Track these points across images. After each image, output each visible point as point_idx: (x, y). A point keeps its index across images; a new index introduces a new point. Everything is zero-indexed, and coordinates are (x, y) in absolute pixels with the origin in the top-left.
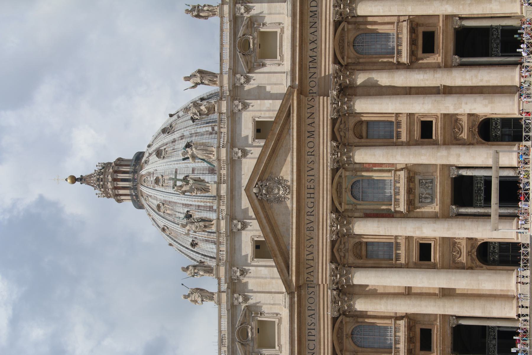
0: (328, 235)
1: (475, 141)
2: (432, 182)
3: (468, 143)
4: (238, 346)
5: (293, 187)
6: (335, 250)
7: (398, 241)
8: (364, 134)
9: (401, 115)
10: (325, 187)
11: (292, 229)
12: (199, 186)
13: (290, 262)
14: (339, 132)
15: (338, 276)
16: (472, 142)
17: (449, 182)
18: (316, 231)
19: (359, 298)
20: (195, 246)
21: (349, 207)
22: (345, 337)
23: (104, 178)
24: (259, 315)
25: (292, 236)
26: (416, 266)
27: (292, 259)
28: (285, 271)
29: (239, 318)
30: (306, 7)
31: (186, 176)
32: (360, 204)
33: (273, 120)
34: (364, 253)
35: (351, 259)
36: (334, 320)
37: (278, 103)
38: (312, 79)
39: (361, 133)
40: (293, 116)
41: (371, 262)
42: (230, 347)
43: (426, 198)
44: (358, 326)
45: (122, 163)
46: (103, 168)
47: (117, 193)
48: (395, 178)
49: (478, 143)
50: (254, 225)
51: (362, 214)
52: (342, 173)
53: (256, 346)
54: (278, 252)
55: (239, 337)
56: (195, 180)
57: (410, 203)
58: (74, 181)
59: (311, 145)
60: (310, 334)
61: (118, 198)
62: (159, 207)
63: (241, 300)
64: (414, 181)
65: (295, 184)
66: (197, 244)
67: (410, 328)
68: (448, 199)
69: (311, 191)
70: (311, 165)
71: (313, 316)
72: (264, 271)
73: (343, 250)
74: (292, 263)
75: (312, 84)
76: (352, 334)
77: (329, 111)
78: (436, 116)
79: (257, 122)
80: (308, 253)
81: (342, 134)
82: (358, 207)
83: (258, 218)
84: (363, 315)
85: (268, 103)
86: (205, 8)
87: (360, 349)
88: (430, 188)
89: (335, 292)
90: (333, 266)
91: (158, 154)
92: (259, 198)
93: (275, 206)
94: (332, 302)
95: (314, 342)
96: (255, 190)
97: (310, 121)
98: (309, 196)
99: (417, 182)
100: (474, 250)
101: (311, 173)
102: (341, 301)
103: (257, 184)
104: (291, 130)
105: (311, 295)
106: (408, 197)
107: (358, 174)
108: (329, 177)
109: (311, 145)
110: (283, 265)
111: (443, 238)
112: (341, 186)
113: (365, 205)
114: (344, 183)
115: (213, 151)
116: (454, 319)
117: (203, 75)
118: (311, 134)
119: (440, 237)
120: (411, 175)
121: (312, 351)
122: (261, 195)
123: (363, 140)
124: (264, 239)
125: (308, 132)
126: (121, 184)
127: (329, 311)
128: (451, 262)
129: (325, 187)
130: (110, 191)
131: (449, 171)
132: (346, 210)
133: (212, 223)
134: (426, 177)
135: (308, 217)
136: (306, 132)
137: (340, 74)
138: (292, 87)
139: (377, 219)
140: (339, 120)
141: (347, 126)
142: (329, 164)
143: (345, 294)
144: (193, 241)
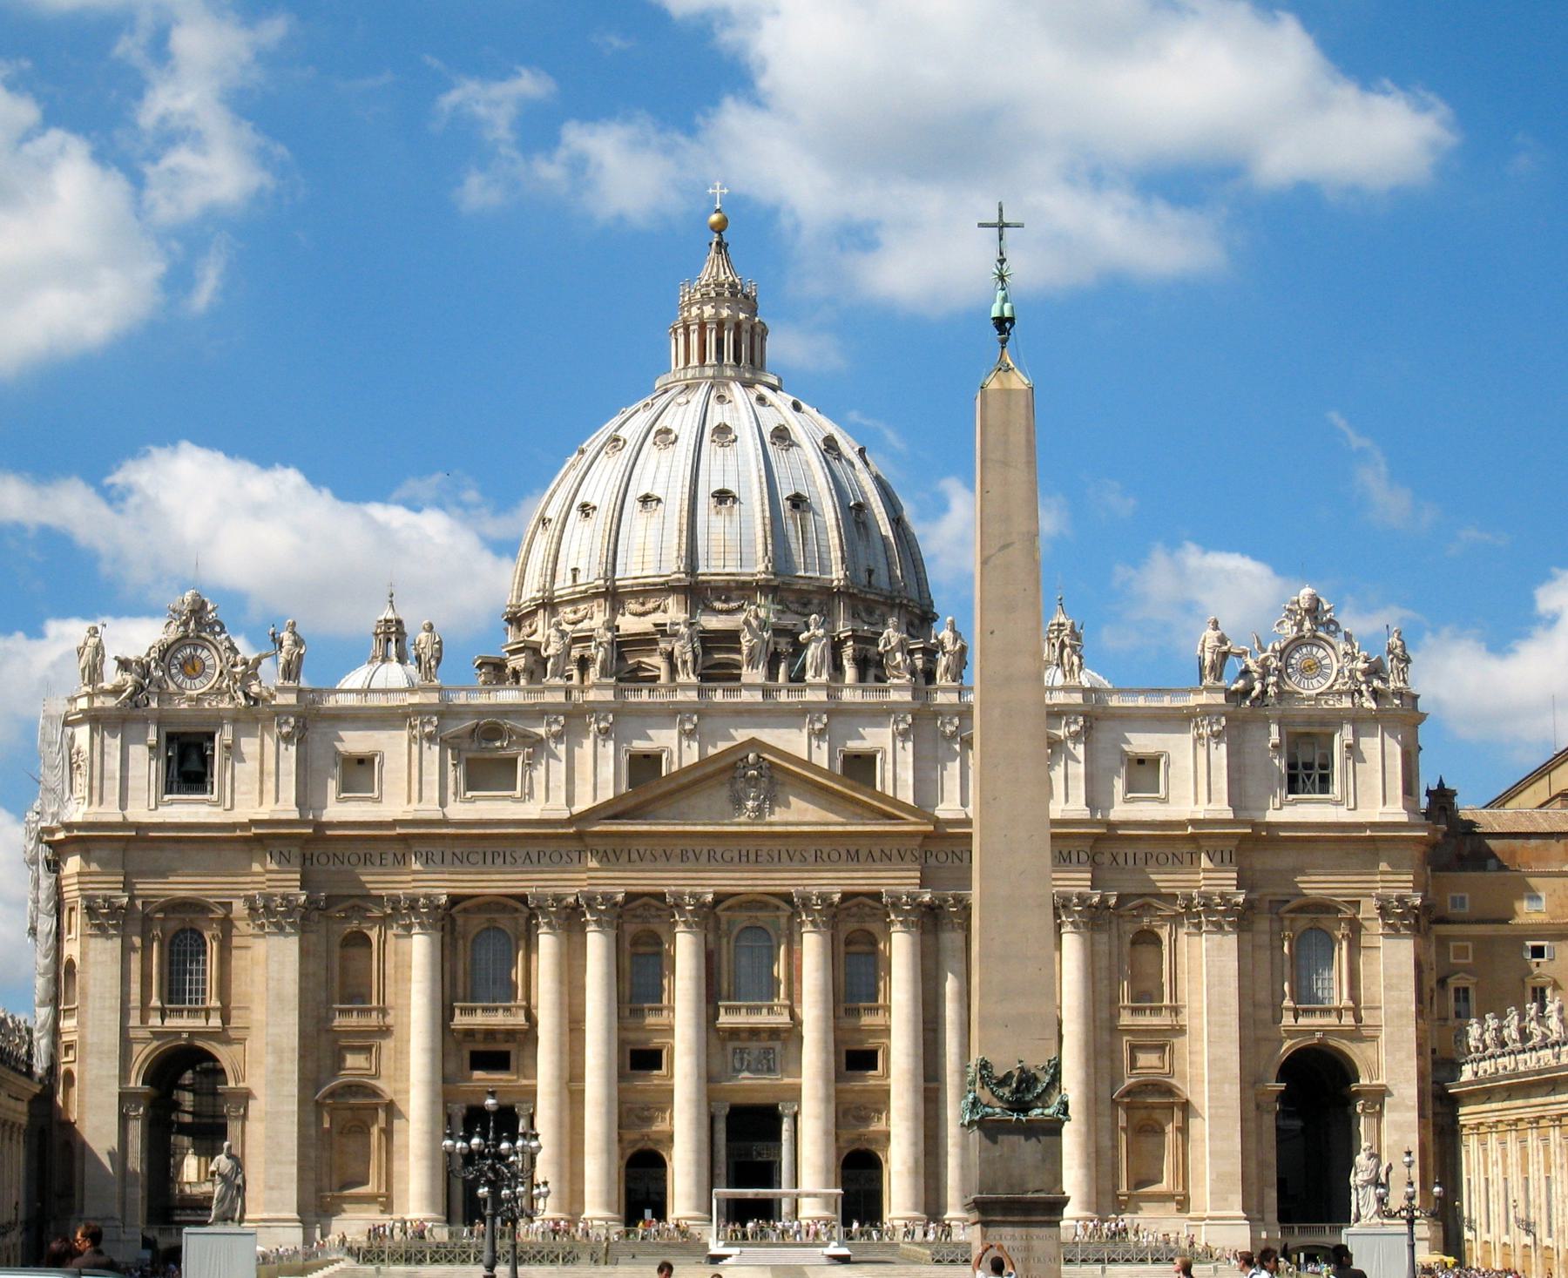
0: (673, 888)
1: (842, 1144)
2: (770, 1070)
3: (839, 1131)
4: (470, 723)
5: (758, 825)
6: (645, 899)
7: (665, 1013)
8: (853, 949)
9: (887, 1014)
10: (760, 882)
11: (684, 824)
12: (757, 651)
13: (625, 821)
14: (857, 905)
15: (603, 907)
16: (841, 1140)
17: (770, 1101)
18: (682, 866)
19: (561, 945)
20: (583, 511)
21: (724, 926)
22: (489, 916)
23: (726, 300)
24: (526, 762)
25: (672, 824)
26: (622, 1043)
27: (632, 824)
28: (610, 812)
29: (520, 725)
30: (1076, 844)
31: (734, 497)
32: (728, 943)
33: (879, 788)
34: (642, 949)
35: (631, 928)
36: (522, 899)
37: (907, 796)
38: (950, 855)
39: (855, 943)
40: (885, 824)
41: (627, 963)
42: (468, 709)
43: (742, 1059)
44: (509, 938)
45: (757, 340)
46: (746, 297)
47: (692, 328)
48: (777, 1005)
49: (838, 1149)
50: (692, 755)
51: (711, 946)
52: (784, 910)
53: (470, 755)
54: (642, 798)
55: (485, 724)
56: (768, 642)
57: (734, 1033)
58: (716, 229)
59: (835, 856)
60: (496, 854)
61: (681, 331)
62: (668, 431)
63: (555, 728)
64: (772, 1040)
65: (766, 829)
66: (587, 515)
67: (511, 1034)
68: (740, 1099)
69: (752, 857)
70: (797, 857)
71: (528, 861)
72: (607, 771)
73: (646, 913)
74: (623, 824)
75: (942, 857)
76: (495, 928)
77: (894, 888)
78: (887, 1074)
79: (874, 757)
80: (642, 852)
81: (854, 910)
82: (724, 941)
83: (704, 761)
84: (531, 947)
85: (907, 776)
86: (1075, 659)
87: (469, 944)
88: (760, 1066)
89: (571, 900)
90: (620, 897)
91: (781, 430)
92: (739, 763)
93: (724, 793)
94: (555, 895)
95: (481, 862)
96: (751, 756)
97: (877, 854)
98: (744, 852)
99: (769, 1044)
100: (651, 1145)
101: (784, 856)
102: (557, 911)
103: (764, 759)
104: (861, 822)
105: (565, 857)
106: (745, 1030)
107: (784, 940)
108: (778, 888)
109: (835, 856)
110: (619, 808)
111: (672, 1091)
112: (761, 909)
113: (728, 953)
114: (767, 914)
115: (820, 676)
116: (529, 1110)
117: (957, 656)
118: (854, 857)
119: (673, 1085)
120: (783, 1035)
121: (465, 860)
122: (744, 767)
123: (842, 947)
124: (664, 774)
125: (857, 851)
126: (711, 339)
127: (539, 889)
128: (628, 1105)
129: (760, 882)
130: (695, 311)
131: (791, 1101)
132: (718, 920)
133: (691, 675)
134: (778, 1061)
135: (705, 852)
136: (856, 848)
137: (960, 907)
138: (937, 822)
139: (704, 975)
140: (878, 905)
141: (867, 919)
142: (800, 888)
143: (568, 918)
144: (594, 508)
